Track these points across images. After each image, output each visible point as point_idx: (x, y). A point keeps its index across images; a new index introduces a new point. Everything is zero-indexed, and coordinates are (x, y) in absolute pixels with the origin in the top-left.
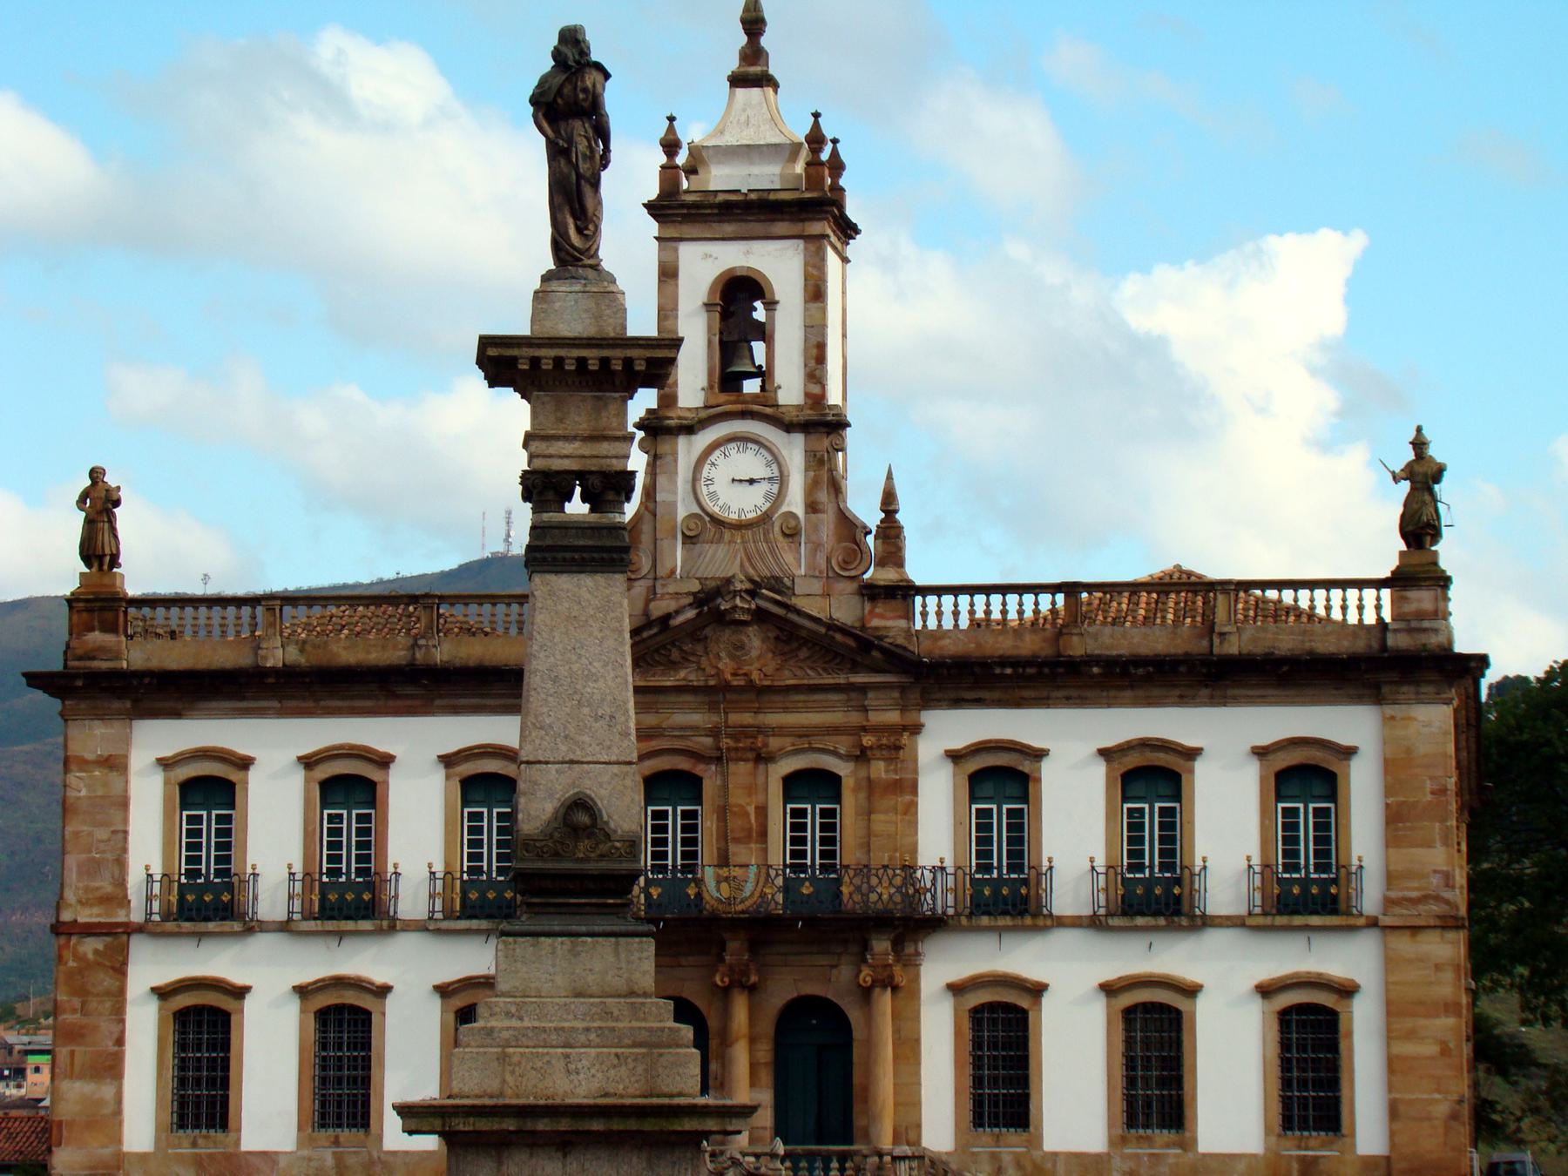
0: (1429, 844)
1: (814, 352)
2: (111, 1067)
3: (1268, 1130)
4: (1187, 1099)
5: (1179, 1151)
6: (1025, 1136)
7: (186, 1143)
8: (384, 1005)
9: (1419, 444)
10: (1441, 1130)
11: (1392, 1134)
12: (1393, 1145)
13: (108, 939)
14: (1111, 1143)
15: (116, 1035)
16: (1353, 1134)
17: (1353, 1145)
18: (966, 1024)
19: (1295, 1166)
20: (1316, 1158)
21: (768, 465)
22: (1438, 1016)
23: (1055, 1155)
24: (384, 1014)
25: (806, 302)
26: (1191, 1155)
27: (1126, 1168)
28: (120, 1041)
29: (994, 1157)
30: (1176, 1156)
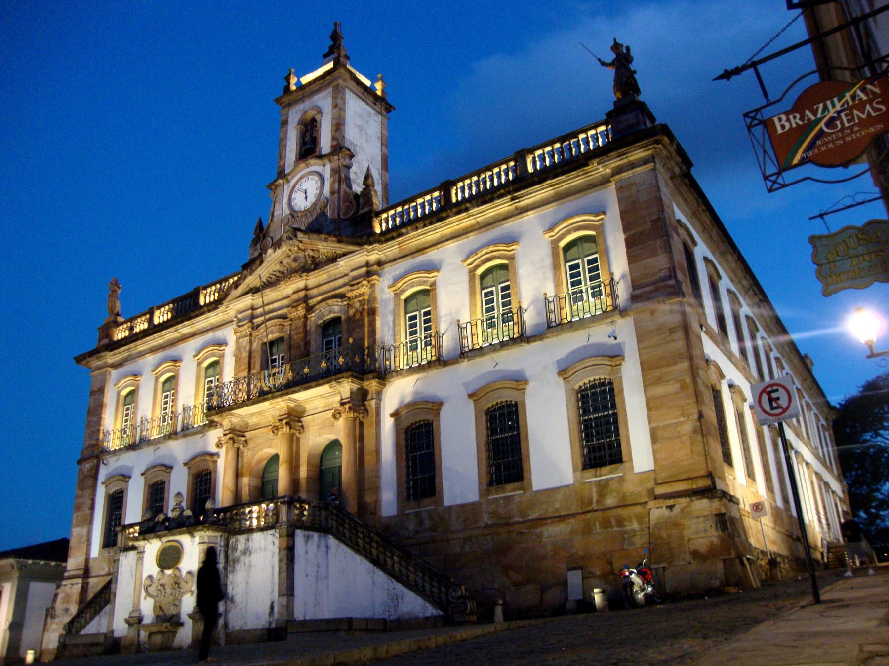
0: (654, 254)
1: (335, 128)
2: (89, 521)
3: (575, 471)
4: (523, 457)
5: (522, 492)
6: (433, 499)
7: (107, 552)
8: (170, 476)
9: (616, 47)
10: (688, 443)
11: (654, 452)
12: (656, 460)
13: (91, 464)
14: (481, 495)
15: (89, 505)
16: (631, 460)
17: (632, 467)
18: (403, 436)
19: (594, 490)
20: (608, 480)
21: (316, 182)
22: (676, 363)
23: (450, 507)
24: (169, 481)
25: (333, 109)
26: (528, 494)
27: (493, 507)
28: (92, 508)
29: (417, 514)
30: (520, 496)
